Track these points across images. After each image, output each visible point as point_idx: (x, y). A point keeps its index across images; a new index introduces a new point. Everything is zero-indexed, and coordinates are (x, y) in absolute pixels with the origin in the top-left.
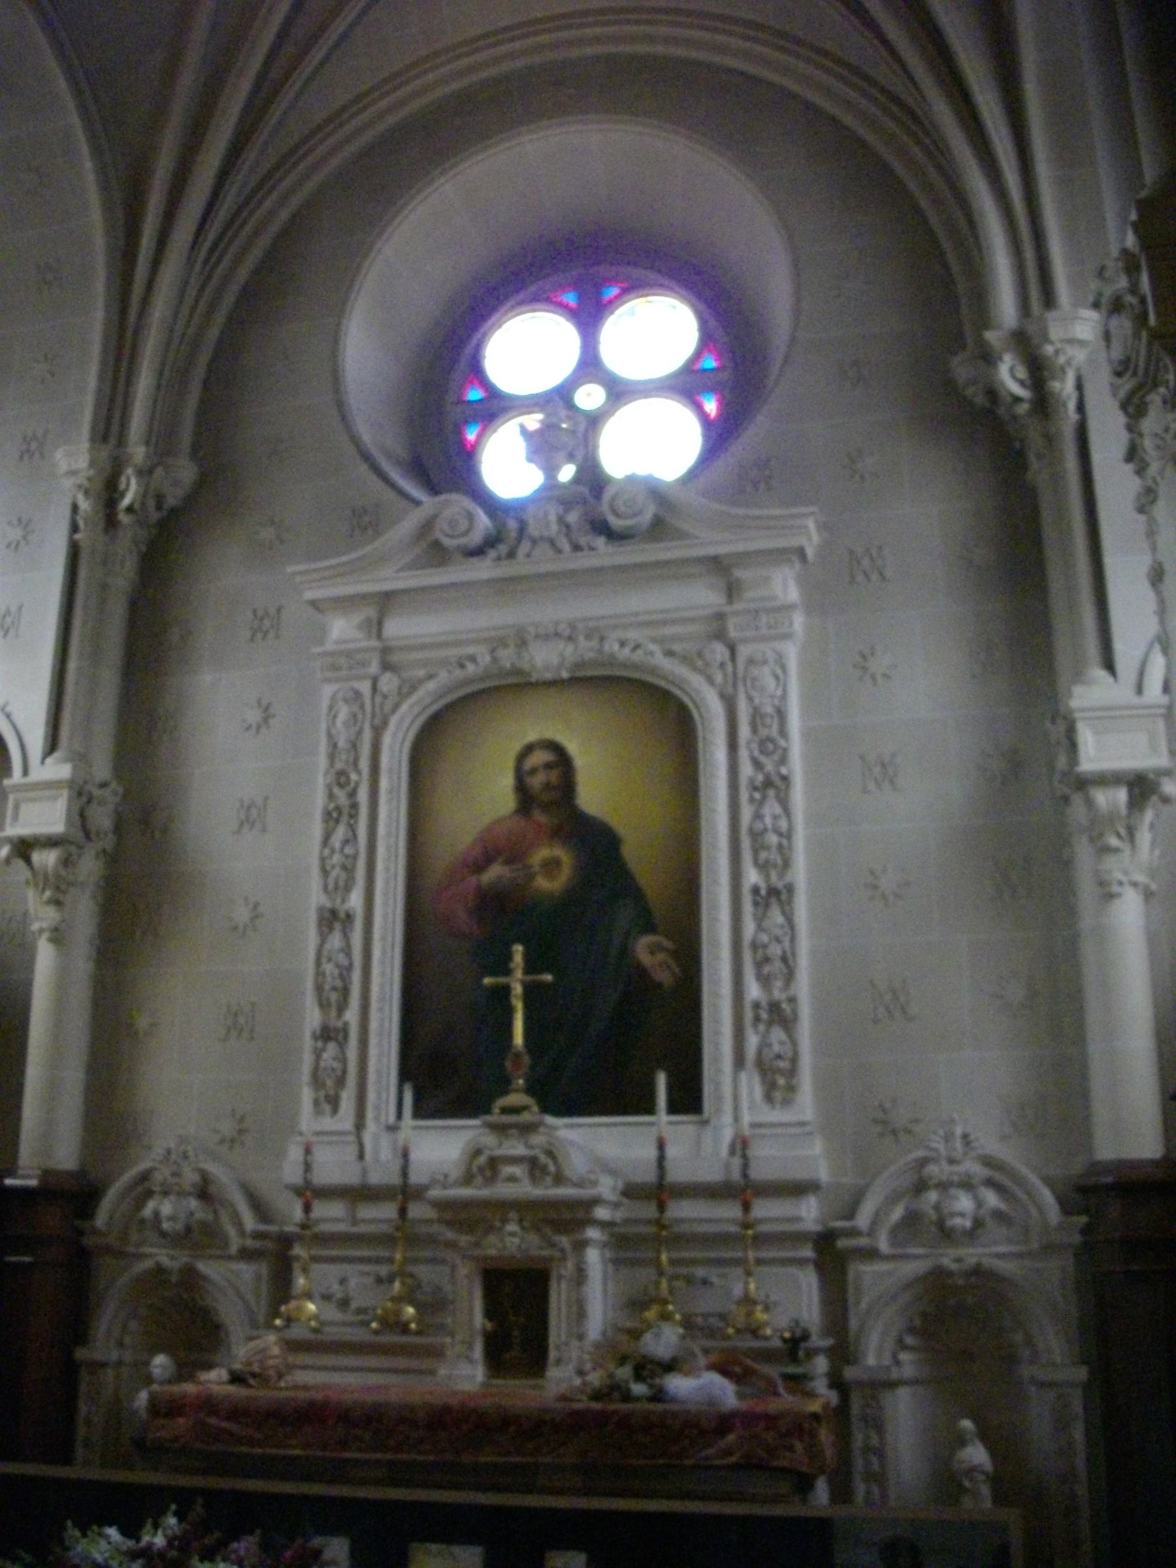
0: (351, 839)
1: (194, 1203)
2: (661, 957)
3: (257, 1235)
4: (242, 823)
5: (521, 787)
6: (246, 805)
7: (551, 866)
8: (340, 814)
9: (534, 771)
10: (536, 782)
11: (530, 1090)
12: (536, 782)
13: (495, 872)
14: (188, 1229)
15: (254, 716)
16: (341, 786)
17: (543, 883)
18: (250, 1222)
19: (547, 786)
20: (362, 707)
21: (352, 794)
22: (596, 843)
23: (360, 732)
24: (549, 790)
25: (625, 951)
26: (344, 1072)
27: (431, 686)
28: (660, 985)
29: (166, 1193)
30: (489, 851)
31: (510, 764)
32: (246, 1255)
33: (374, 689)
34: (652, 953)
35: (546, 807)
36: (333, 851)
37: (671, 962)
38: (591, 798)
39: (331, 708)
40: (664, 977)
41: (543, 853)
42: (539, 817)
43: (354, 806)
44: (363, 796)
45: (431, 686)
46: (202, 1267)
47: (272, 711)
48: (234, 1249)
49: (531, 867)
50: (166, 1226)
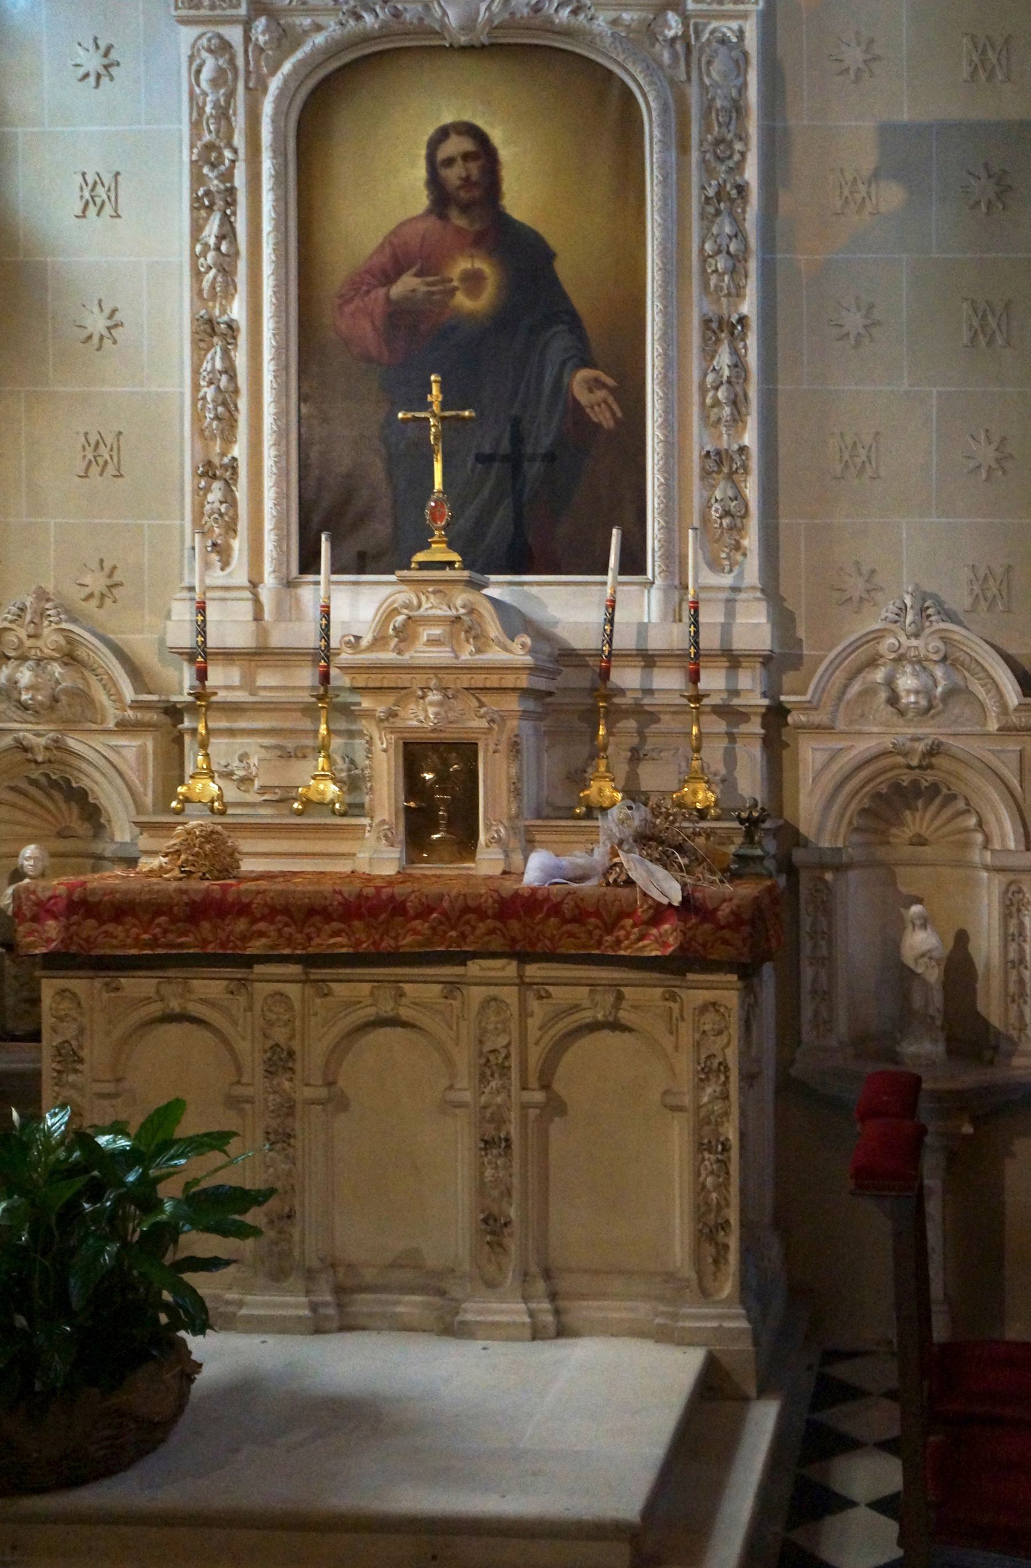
0: (228, 233)
1: (57, 669)
2: (601, 394)
3: (136, 705)
4: (87, 203)
5: (434, 181)
6: (90, 180)
7: (473, 281)
8: (212, 204)
9: (449, 162)
10: (453, 175)
11: (451, 545)
12: (453, 175)
13: (406, 284)
14: (55, 699)
15: (93, 62)
16: (213, 166)
17: (463, 301)
18: (129, 694)
19: (466, 181)
20: (232, 61)
21: (227, 176)
22: (524, 256)
23: (231, 95)
24: (467, 185)
25: (560, 387)
26: (235, 519)
27: (320, 39)
28: (598, 426)
29: (23, 658)
30: (396, 259)
31: (423, 152)
32: (124, 727)
33: (247, 39)
34: (591, 390)
35: (465, 208)
36: (206, 246)
37: (611, 400)
38: (521, 198)
39: (191, 58)
40: (603, 417)
41: (463, 265)
42: (458, 220)
43: (232, 191)
44: (240, 179)
45: (320, 39)
46: (72, 743)
47: (114, 55)
48: (111, 725)
49: (452, 280)
50: (25, 697)
